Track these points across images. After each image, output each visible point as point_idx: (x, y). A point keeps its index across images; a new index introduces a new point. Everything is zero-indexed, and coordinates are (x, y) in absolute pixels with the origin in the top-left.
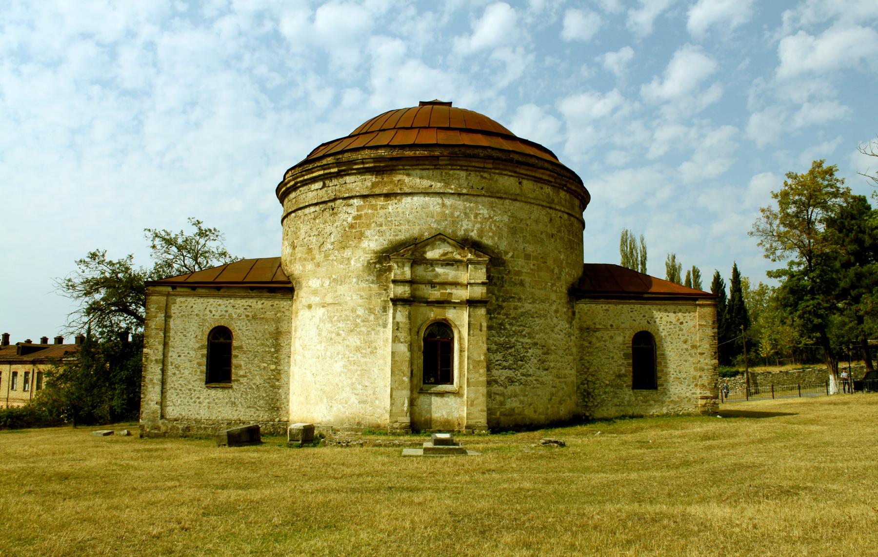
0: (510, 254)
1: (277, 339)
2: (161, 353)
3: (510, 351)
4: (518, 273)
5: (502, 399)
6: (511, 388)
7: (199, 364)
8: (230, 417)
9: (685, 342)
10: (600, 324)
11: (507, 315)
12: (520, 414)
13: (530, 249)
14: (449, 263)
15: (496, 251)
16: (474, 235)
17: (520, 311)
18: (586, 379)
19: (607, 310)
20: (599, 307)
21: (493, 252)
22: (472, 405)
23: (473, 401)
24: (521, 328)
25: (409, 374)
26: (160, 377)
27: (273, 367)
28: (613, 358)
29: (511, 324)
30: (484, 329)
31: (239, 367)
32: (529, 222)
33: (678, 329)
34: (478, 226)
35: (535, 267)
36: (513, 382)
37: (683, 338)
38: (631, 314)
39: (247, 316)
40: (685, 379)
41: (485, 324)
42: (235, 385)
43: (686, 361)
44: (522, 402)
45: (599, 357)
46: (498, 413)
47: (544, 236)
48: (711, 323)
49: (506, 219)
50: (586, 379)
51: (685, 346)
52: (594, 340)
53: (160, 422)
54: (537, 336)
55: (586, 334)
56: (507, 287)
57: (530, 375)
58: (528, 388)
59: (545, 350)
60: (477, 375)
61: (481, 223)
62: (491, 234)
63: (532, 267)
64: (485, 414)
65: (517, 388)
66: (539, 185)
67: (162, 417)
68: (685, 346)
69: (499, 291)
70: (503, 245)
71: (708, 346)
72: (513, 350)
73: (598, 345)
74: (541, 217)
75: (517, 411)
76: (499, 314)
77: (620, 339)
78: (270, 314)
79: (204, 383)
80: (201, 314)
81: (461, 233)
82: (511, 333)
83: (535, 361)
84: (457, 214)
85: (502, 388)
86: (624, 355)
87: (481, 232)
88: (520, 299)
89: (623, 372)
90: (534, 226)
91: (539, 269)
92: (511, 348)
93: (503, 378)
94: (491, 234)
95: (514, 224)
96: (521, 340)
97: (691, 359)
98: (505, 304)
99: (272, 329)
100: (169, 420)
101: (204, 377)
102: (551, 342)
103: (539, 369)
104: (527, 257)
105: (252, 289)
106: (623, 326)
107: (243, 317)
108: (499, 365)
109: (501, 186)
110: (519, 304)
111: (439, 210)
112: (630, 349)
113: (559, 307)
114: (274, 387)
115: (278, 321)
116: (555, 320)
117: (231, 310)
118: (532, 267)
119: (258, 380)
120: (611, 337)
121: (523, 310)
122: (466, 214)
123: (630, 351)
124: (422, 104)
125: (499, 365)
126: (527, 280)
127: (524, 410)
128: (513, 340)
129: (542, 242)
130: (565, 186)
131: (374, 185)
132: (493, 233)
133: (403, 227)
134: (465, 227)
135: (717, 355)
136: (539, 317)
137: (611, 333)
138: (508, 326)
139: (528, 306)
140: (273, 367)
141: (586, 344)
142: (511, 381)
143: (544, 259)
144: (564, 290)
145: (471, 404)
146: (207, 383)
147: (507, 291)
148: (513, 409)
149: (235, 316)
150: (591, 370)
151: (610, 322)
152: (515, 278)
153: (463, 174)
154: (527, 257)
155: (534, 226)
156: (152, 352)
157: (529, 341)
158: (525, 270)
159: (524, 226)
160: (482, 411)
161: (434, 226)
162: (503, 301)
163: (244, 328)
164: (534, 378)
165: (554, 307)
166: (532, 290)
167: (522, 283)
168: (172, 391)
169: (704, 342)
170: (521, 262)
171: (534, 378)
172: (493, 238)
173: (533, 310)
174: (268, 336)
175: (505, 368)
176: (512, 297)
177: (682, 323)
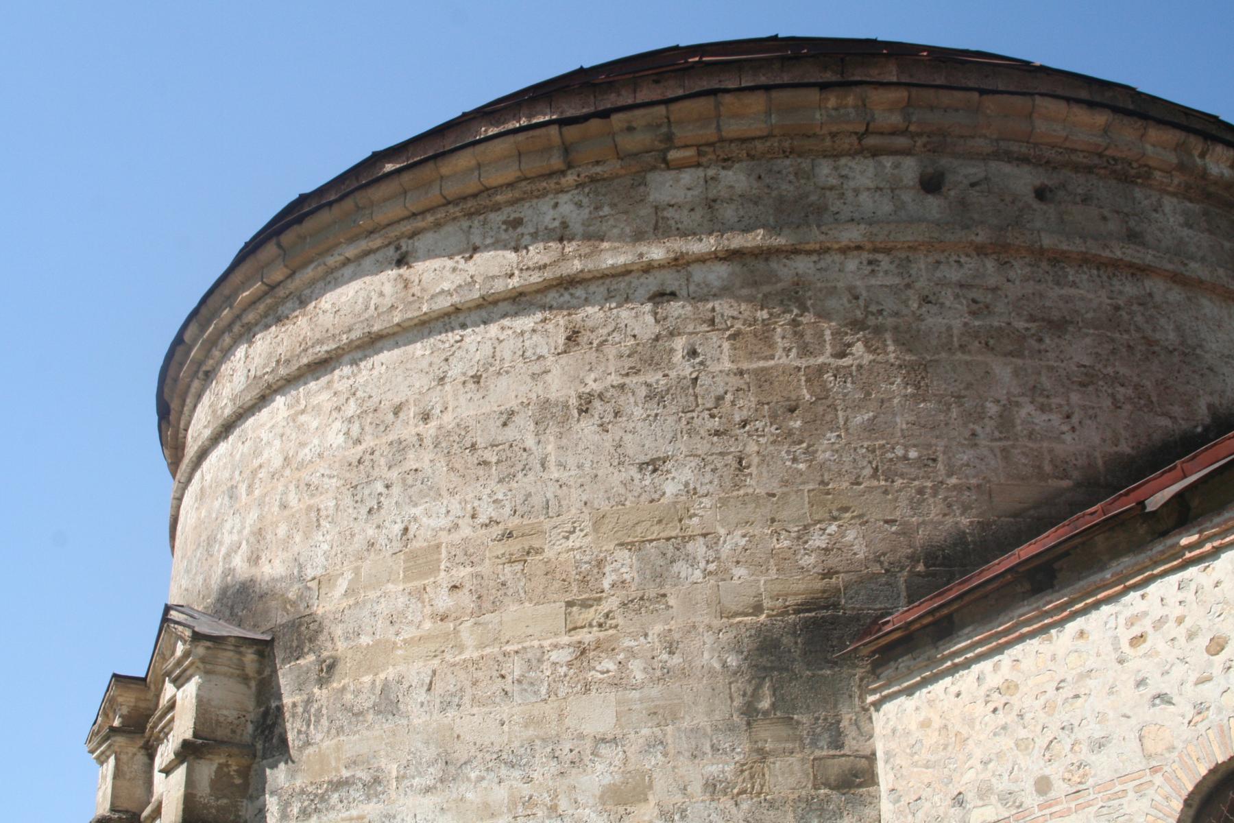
0: (342, 585)
13: (430, 520)
19: (1009, 687)
20: (966, 680)
32: (435, 400)
35: (466, 599)
38: (1138, 662)
47: (523, 431)
63: (444, 601)
66: (496, 218)
69: (292, 775)
74: (506, 351)
88: (374, 785)
91: (487, 599)
95: (369, 442)
104: (420, 562)
106: (1103, 765)
113: (654, 760)
144: (710, 652)
151: (1032, 765)
154: (420, 562)
155: (461, 407)
165: (600, 775)
176: (338, 785)
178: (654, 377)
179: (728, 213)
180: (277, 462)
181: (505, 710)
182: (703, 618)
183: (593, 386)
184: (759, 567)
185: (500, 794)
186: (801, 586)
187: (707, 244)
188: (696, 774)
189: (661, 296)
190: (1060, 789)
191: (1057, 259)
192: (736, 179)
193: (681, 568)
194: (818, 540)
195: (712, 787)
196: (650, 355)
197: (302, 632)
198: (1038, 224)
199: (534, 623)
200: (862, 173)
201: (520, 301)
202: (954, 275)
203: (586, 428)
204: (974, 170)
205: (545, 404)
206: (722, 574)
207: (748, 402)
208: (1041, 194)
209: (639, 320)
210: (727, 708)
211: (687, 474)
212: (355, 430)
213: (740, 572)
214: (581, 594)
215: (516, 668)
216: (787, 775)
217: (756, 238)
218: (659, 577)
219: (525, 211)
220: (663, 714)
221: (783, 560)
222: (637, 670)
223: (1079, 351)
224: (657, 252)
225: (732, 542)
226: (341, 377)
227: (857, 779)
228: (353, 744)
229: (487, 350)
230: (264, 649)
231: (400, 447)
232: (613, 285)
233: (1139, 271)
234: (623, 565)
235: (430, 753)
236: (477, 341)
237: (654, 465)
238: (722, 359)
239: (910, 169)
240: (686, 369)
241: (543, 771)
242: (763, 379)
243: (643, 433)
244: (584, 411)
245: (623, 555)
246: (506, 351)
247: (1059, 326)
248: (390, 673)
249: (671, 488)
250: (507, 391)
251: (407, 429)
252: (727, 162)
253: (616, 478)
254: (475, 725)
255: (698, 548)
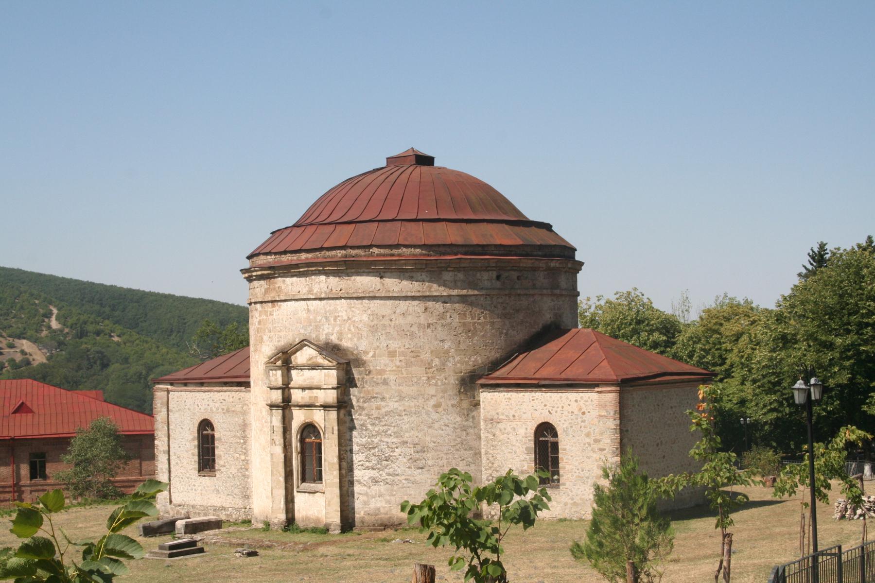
0: (371, 354)
1: (244, 431)
2: (166, 445)
3: (373, 451)
4: (381, 372)
5: (365, 498)
6: (375, 488)
7: (193, 455)
8: (216, 504)
9: (588, 435)
10: (503, 414)
11: (368, 415)
12: (386, 514)
13: (394, 345)
14: (314, 367)
15: (355, 352)
16: (334, 339)
17: (383, 410)
18: (491, 475)
21: (353, 354)
22: (329, 505)
23: (329, 502)
24: (385, 428)
25: (283, 474)
26: (167, 466)
27: (243, 457)
28: (515, 452)
29: (373, 424)
30: (336, 432)
31: (220, 457)
32: (393, 317)
33: (580, 420)
34: (337, 329)
35: (403, 364)
36: (377, 482)
37: (586, 431)
38: (532, 403)
39: (223, 409)
40: (588, 478)
41: (336, 428)
42: (217, 473)
43: (588, 458)
44: (389, 502)
45: (503, 451)
46: (362, 513)
47: (415, 329)
48: (612, 413)
49: (365, 317)
50: (491, 475)
51: (588, 440)
52: (498, 433)
53: (169, 506)
54: (407, 435)
55: (490, 426)
56: (367, 387)
57: (398, 475)
58: (395, 488)
59: (419, 448)
60: (332, 477)
61: (340, 326)
62: (350, 336)
63: (398, 363)
64: (339, 514)
65: (382, 488)
67: (171, 502)
68: (588, 440)
69: (360, 392)
70: (363, 346)
71: (609, 441)
72: (376, 450)
73: (502, 437)
74: (411, 309)
75: (382, 511)
76: (360, 415)
77: (522, 431)
78: (238, 408)
79: (197, 472)
80: (192, 409)
81: (323, 338)
82: (374, 433)
83: (405, 460)
84: (319, 318)
85: (365, 488)
86: (527, 449)
87: (340, 334)
88: (383, 399)
89: (525, 468)
90: (401, 321)
91: (408, 364)
92: (374, 448)
93: (366, 478)
94: (350, 336)
95: (375, 322)
96: (386, 440)
97: (594, 455)
98: (365, 405)
99: (241, 421)
100: (176, 506)
101: (197, 466)
102: (428, 439)
103: (409, 468)
104: (392, 354)
105: (226, 384)
106: (525, 416)
107: (220, 410)
108: (362, 465)
109: (359, 285)
110: (383, 404)
111: (305, 315)
112: (533, 442)
114: (244, 476)
115: (244, 413)
116: (435, 416)
117: (212, 404)
118: (398, 363)
119: (234, 470)
120: (514, 429)
121: (387, 409)
122: (326, 318)
123: (532, 445)
124: (390, 160)
125: (362, 465)
126: (392, 377)
127: (391, 510)
128: (376, 440)
129: (412, 336)
130: (449, 266)
131: (267, 291)
132: (352, 334)
133: (283, 334)
134: (326, 331)
135: (618, 452)
136: (409, 414)
137: (514, 424)
138: (370, 427)
139: (393, 405)
140: (243, 457)
141: (491, 437)
142: (375, 481)
143: (416, 354)
144: (453, 380)
145: (328, 504)
146: (199, 471)
147: (369, 392)
148: (379, 509)
149: (214, 410)
150: (496, 465)
151: (512, 413)
152: (379, 378)
153: (323, 277)
154: (392, 354)
155: (401, 321)
156: (160, 444)
157: (395, 440)
158: (389, 369)
159: (387, 323)
160: (336, 511)
161: (302, 331)
162: (364, 402)
163: (221, 421)
164: (403, 477)
165: (432, 402)
166: (398, 387)
167: (385, 382)
168: (177, 479)
169: (605, 435)
170: (385, 360)
171: (403, 477)
172: (351, 339)
173: (400, 408)
174: (238, 428)
175: (368, 468)
176: (373, 398)
177: (584, 413)
178: (443, 322)
179: (459, 284)
180: (346, 318)
181: (412, 388)
182: (452, 373)
183: (430, 322)
184: (462, 364)
185: (412, 404)
186: (470, 368)
187: (455, 292)
188: (450, 403)
189: (445, 302)
190: (517, 417)
191: (519, 295)
192: (460, 276)
193: (448, 363)
194: (473, 359)
195: (452, 405)
196: (442, 317)
197: (360, 363)
198: (517, 287)
199: (418, 370)
200: (485, 276)
201: (413, 298)
202: (500, 300)
203: (429, 331)
204: (507, 274)
205: (420, 324)
206: (455, 365)
207: (461, 329)
208: (519, 278)
209: (439, 307)
210: (456, 391)
211: (449, 344)
212: (371, 318)
213: (459, 365)
214: (429, 366)
215: (415, 380)
216: (465, 404)
217: (464, 292)
218: (444, 364)
219: (414, 274)
220: (444, 391)
221: (467, 363)
222: (439, 383)
223: (521, 316)
224: (445, 294)
225: (457, 358)
226: (366, 301)
227: (477, 405)
228: (377, 389)
229: (406, 308)
230: (348, 364)
231: (384, 325)
232: (435, 299)
233: (533, 295)
234: (437, 361)
235: (396, 394)
236: (403, 305)
237: (443, 341)
238: (456, 319)
239: (494, 274)
240: (449, 320)
241: (421, 400)
242: (464, 324)
243: (441, 333)
244: (429, 327)
245: (437, 359)
246: (411, 309)
247: (518, 311)
248: (386, 376)
249: (446, 347)
250: (410, 319)
251: (386, 322)
252: (459, 271)
253: (436, 343)
254: (406, 390)
255: (451, 359)
